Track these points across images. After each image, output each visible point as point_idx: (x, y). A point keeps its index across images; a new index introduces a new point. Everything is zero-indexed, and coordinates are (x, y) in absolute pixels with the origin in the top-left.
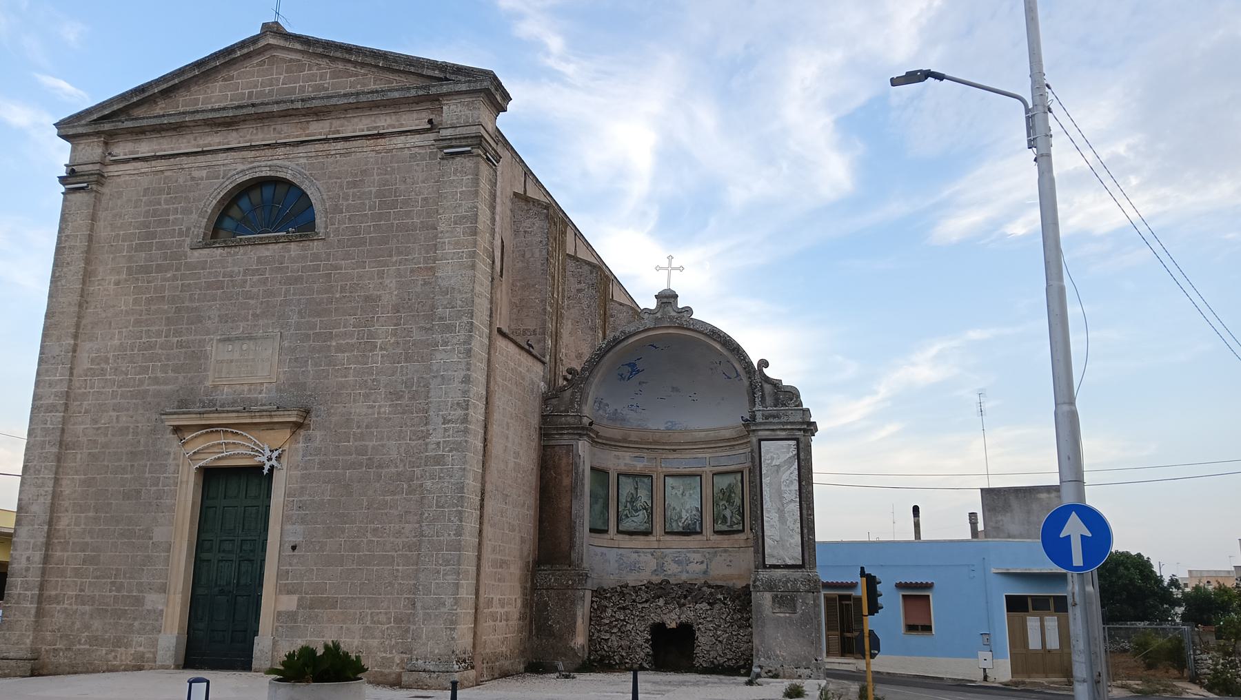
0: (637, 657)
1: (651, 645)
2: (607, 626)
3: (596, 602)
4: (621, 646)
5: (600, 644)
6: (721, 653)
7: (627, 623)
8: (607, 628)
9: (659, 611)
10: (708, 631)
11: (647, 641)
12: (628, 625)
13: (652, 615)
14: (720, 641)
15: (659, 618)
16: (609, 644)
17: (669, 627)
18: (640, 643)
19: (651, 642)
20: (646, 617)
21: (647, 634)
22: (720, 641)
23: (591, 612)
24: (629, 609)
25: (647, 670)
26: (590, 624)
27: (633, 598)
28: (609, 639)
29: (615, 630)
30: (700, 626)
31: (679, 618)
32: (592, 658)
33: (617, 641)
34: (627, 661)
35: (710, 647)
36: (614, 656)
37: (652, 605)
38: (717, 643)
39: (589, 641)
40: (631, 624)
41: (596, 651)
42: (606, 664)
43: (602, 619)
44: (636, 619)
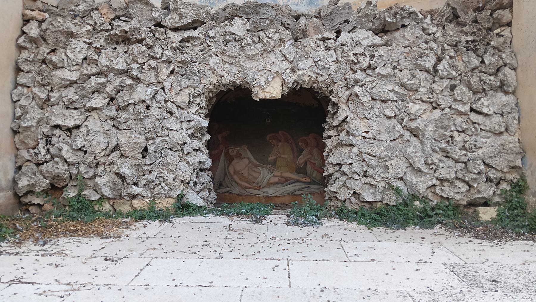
0: (170, 177)
1: (209, 145)
2: (72, 90)
3: (41, 22)
4: (117, 147)
5: (48, 142)
6: (420, 164)
7: (137, 80)
8: (71, 94)
9: (233, 48)
10: (379, 104)
11: (196, 134)
12: (140, 87)
13: (213, 61)
14: (415, 133)
15: (234, 69)
16: (80, 142)
17: (262, 96)
18: (178, 137)
19: (208, 137)
20: (195, 67)
21: (198, 113)
22: (415, 133)
23: (21, 48)
24: (140, 41)
25: (198, 210)
26: (16, 85)
27: (156, 14)
28: (78, 127)
29: (98, 101)
30: (356, 89)
31: (293, 70)
32: (23, 182)
33: (107, 134)
34: (136, 190)
35: (388, 148)
36: (95, 176)
37: (211, 33)
38: (407, 135)
39: (15, 132)
40: (148, 85)
41: (38, 164)
42: (69, 200)
43: (56, 67)
44: (165, 70)
